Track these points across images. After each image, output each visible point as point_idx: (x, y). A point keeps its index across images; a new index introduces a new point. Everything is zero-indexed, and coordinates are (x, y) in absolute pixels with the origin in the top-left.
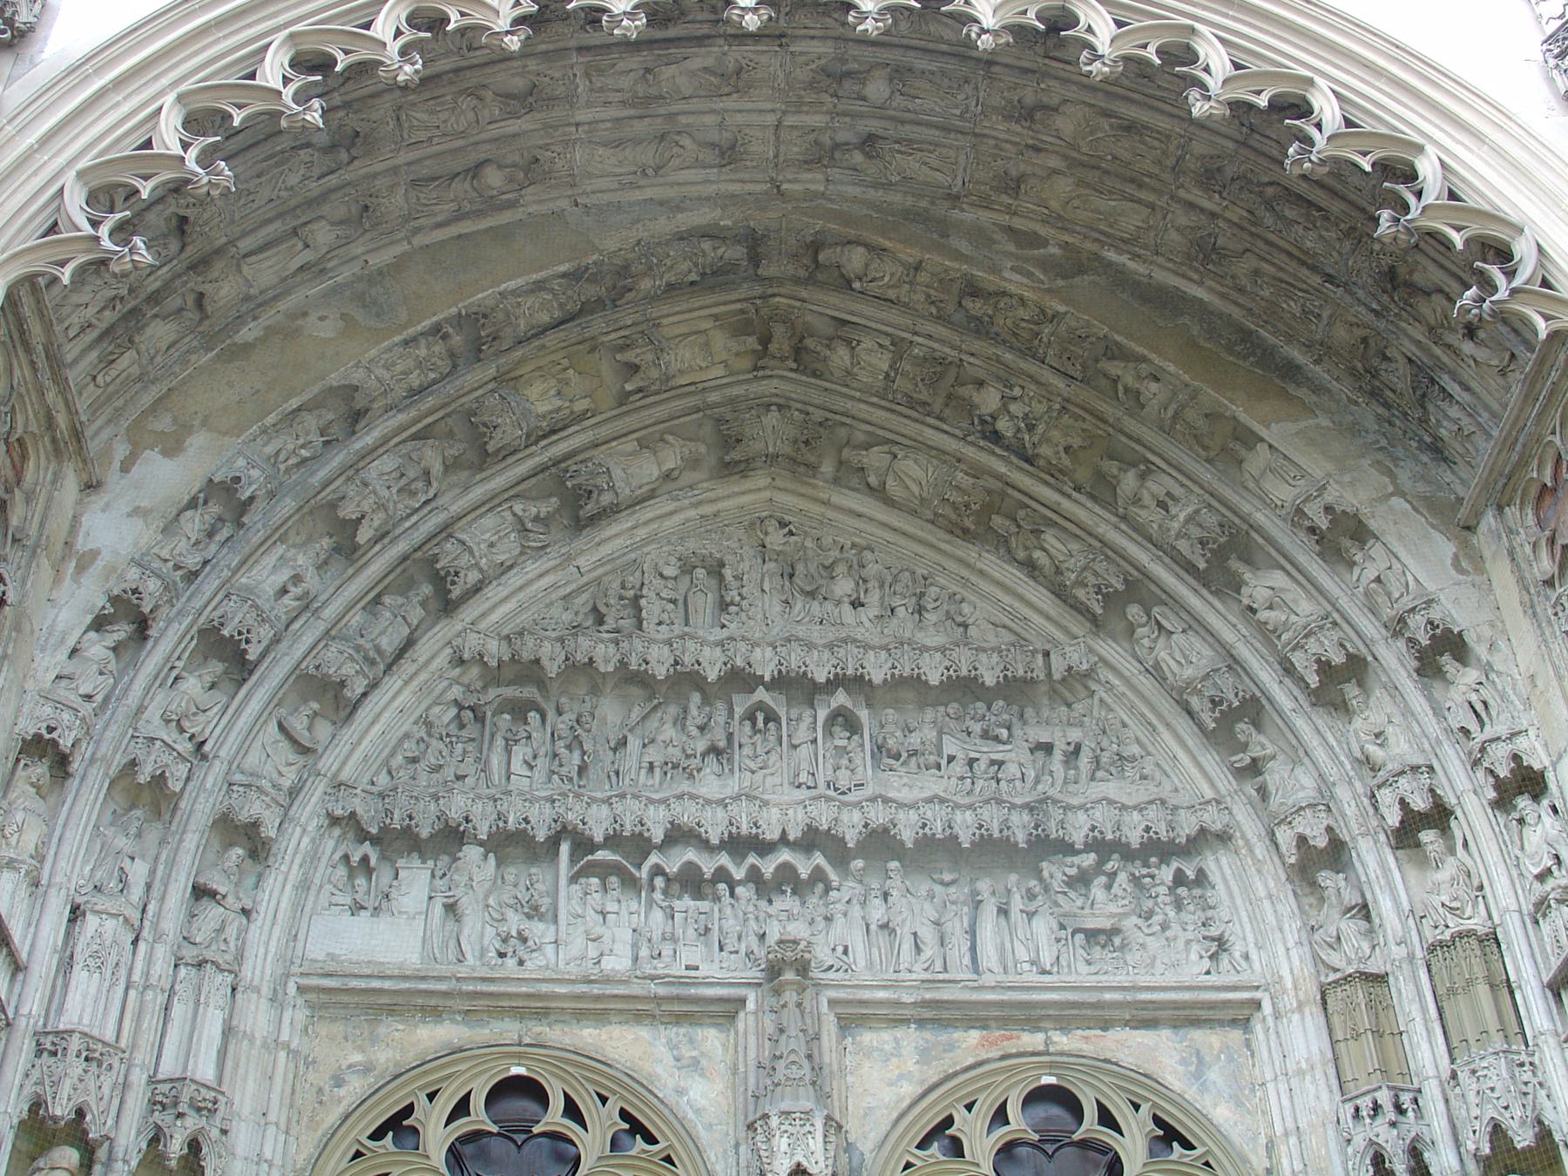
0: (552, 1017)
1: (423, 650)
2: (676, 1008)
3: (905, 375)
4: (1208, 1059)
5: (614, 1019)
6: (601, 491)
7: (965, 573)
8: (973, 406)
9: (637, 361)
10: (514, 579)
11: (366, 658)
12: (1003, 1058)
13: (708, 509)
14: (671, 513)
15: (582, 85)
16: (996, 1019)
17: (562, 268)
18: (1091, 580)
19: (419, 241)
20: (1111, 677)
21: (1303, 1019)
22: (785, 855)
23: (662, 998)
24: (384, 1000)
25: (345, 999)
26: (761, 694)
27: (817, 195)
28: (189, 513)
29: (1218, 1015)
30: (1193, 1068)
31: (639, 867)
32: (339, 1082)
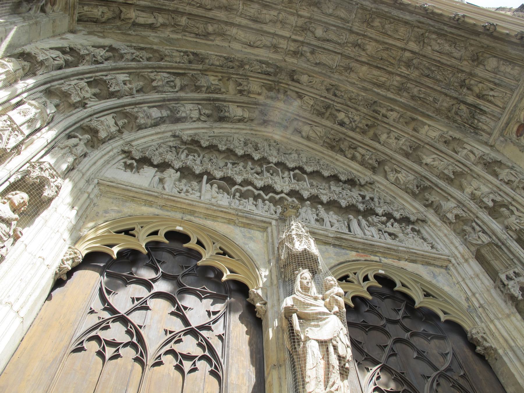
0: (196, 215)
1: (163, 128)
2: (244, 221)
3: (318, 105)
4: (436, 274)
5: (219, 220)
6: (225, 111)
7: (332, 160)
8: (336, 117)
9: (242, 83)
10: (195, 125)
11: (146, 115)
12: (365, 260)
13: (253, 132)
14: (243, 129)
15: (241, 7)
16: (362, 249)
17: (225, 55)
18: (374, 157)
19: (184, 37)
20: (380, 186)
21: (469, 264)
22: (283, 195)
23: (240, 216)
24: (131, 194)
25: (115, 191)
26: (271, 165)
27: (295, 63)
28: (102, 49)
29: (436, 263)
30: (432, 275)
31: (231, 189)
32: (106, 212)
